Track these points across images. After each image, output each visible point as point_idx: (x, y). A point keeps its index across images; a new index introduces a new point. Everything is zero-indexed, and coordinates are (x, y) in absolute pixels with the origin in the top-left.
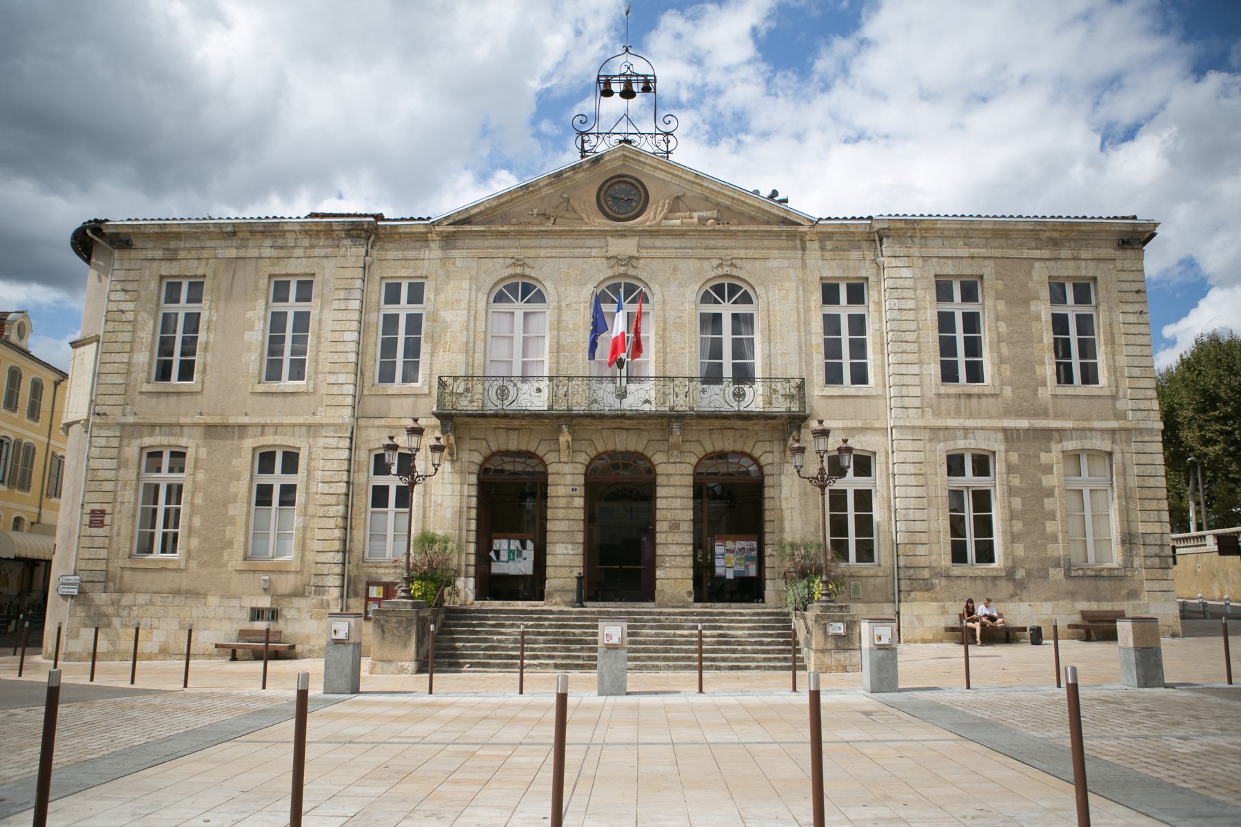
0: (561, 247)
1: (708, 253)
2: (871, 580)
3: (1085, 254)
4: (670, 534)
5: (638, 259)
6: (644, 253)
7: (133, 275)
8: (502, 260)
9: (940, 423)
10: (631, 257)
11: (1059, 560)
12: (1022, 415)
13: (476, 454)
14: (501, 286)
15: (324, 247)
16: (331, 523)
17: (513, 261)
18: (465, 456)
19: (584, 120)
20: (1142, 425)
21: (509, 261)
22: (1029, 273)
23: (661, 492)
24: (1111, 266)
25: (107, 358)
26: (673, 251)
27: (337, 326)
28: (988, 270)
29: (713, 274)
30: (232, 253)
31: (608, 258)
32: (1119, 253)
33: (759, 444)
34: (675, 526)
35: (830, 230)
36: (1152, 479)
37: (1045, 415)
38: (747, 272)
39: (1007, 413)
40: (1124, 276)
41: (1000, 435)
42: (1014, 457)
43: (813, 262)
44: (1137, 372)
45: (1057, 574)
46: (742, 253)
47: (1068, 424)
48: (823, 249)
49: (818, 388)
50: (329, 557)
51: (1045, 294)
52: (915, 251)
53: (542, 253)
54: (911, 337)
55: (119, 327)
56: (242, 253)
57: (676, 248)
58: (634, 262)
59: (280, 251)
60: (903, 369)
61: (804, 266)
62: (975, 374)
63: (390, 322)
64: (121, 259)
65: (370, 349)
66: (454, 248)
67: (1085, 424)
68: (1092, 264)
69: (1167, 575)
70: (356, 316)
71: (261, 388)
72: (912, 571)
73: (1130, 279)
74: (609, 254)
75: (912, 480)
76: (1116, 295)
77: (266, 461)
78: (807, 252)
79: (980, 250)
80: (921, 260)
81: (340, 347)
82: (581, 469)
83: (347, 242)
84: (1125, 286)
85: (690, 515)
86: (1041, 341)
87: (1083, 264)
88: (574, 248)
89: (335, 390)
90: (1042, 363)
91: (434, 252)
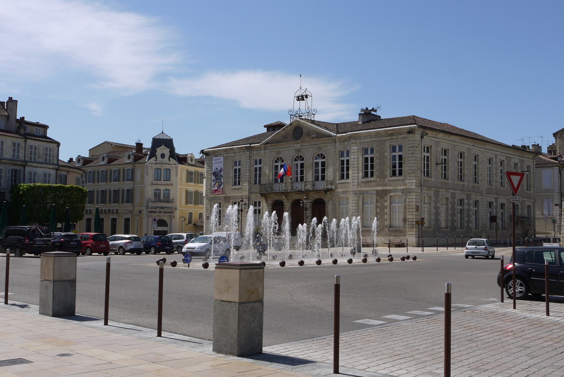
0: (286, 148)
6: (302, 147)
10: (299, 149)
11: (387, 226)
12: (381, 186)
13: (271, 201)
14: (276, 159)
18: (269, 201)
24: (407, 140)
26: (308, 146)
29: (315, 152)
31: (295, 150)
32: (408, 135)
36: (412, 203)
37: (386, 185)
39: (377, 186)
40: (410, 143)
44: (410, 172)
45: (386, 229)
53: (282, 149)
61: (335, 147)
63: (256, 168)
65: (252, 177)
68: (401, 140)
69: (413, 230)
71: (233, 187)
73: (411, 143)
82: (290, 204)
83: (246, 151)
84: (410, 146)
86: (387, 164)
90: (387, 171)
91: (262, 151)
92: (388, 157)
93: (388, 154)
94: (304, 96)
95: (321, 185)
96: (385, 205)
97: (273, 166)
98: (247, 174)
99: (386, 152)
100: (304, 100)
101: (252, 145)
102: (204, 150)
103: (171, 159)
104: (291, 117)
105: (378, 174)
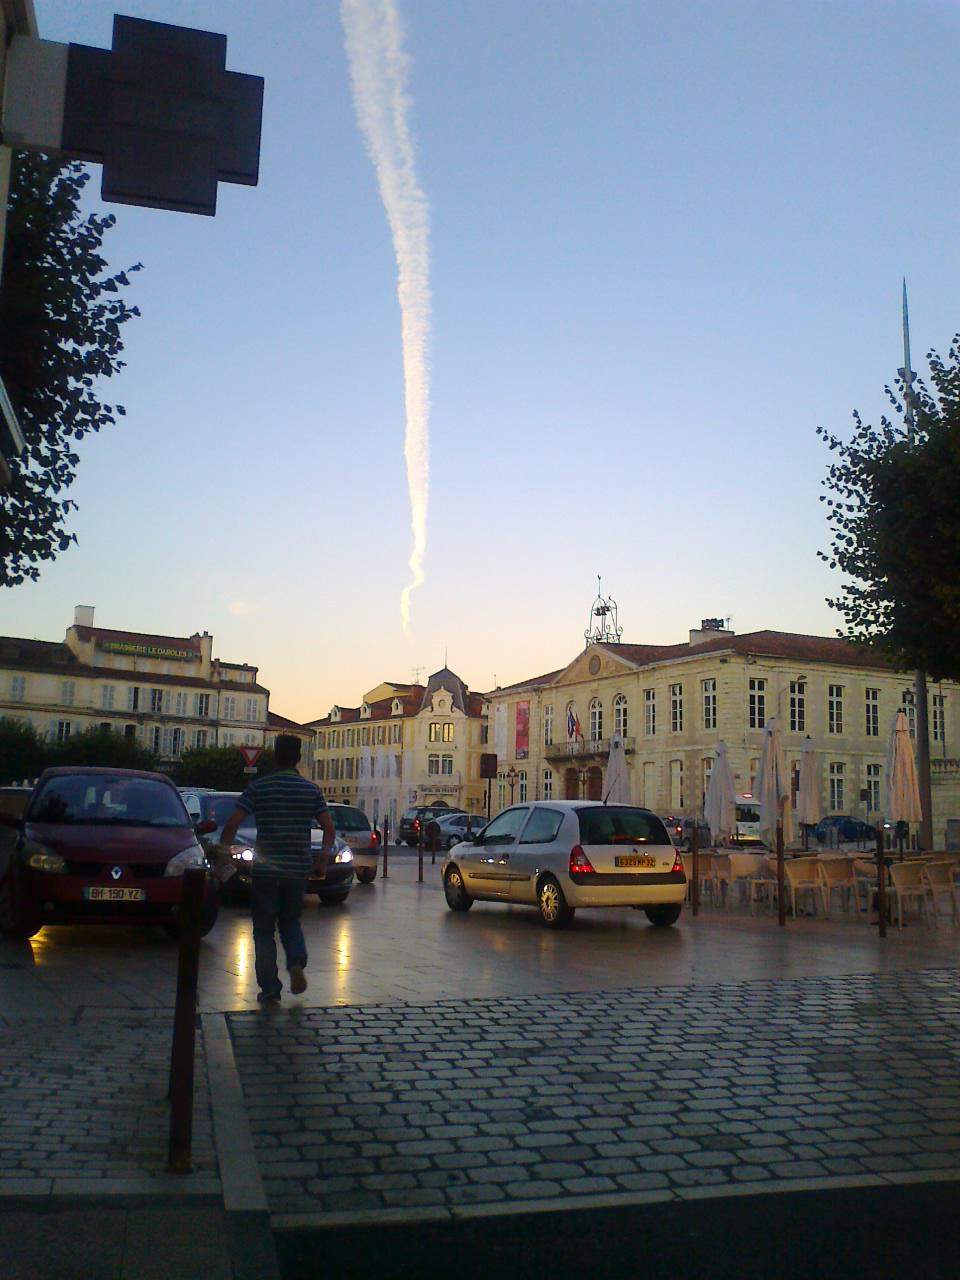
37: (695, 743)
47: (703, 747)
51: (698, 686)
92: (699, 700)
103: (454, 709)
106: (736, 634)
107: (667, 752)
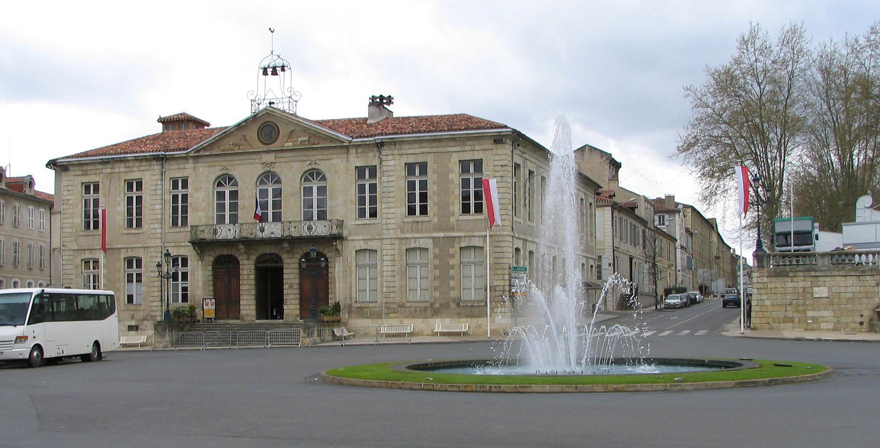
1: (304, 158)
2: (373, 309)
3: (477, 148)
4: (289, 290)
5: (275, 163)
6: (278, 160)
7: (71, 183)
8: (218, 167)
9: (403, 236)
15: (145, 166)
16: (156, 289)
17: (223, 167)
19: (252, 93)
20: (498, 233)
21: (221, 167)
22: (449, 159)
23: (285, 271)
25: (65, 221)
26: (290, 158)
27: (152, 202)
28: (430, 159)
30: (109, 171)
33: (326, 249)
34: (291, 287)
35: (358, 143)
36: (501, 260)
37: (452, 230)
38: (322, 166)
40: (497, 157)
41: (431, 240)
42: (437, 251)
43: (353, 159)
45: (453, 305)
46: (320, 157)
47: (463, 234)
48: (357, 152)
49: (352, 221)
50: (155, 304)
51: (457, 169)
52: (396, 152)
53: (235, 163)
54: (392, 195)
55: (68, 207)
56: (113, 171)
57: (291, 157)
58: (273, 165)
59: (127, 169)
60: (388, 211)
62: (424, 211)
63: (175, 198)
64: (66, 176)
65: (167, 212)
66: (199, 163)
67: (471, 234)
68: (481, 152)
70: (160, 197)
71: (125, 232)
72: (388, 305)
74: (263, 162)
75: (390, 263)
76: (492, 167)
77: (129, 262)
78: (349, 155)
79: (425, 149)
80: (399, 156)
81: (155, 212)
82: (253, 262)
84: (497, 163)
85: (298, 281)
87: (476, 153)
88: (248, 160)
89: (153, 231)
90: (453, 204)
93: (456, 177)
94: (278, 67)
95: (320, 229)
96: (450, 263)
97: (213, 192)
98: (158, 207)
99: (452, 172)
100: (277, 74)
101: (167, 153)
102: (58, 161)
104: (252, 105)
105: (437, 210)
106: (395, 116)
107: (401, 239)
